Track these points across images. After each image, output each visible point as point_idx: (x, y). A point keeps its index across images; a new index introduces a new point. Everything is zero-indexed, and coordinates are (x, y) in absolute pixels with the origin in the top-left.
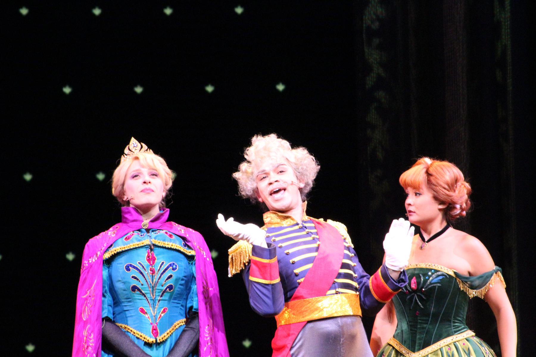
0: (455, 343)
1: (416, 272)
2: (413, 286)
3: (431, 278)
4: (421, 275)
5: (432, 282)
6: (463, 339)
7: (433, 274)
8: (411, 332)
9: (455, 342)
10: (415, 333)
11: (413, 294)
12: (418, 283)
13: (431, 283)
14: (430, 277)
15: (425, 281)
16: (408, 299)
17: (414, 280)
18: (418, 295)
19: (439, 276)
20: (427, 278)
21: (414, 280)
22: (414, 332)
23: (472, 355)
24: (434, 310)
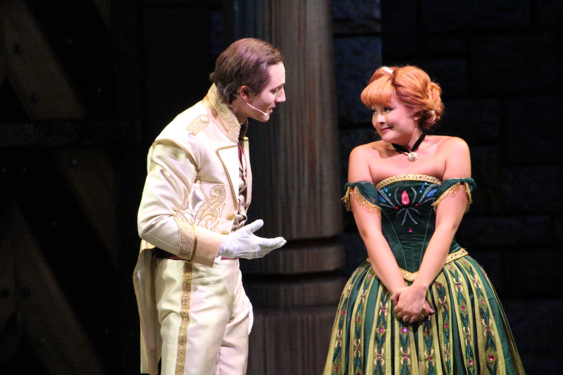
0: (455, 262)
1: (407, 185)
2: (405, 203)
3: (426, 192)
4: (412, 188)
5: (428, 196)
6: (462, 257)
7: (426, 187)
8: (405, 250)
9: (455, 260)
10: (409, 252)
11: (404, 209)
12: (411, 198)
13: (426, 198)
14: (424, 191)
15: (419, 196)
16: (399, 215)
17: (405, 195)
18: (409, 210)
19: (433, 188)
20: (421, 192)
21: (405, 195)
22: (408, 250)
23: (475, 274)
24: (430, 226)
